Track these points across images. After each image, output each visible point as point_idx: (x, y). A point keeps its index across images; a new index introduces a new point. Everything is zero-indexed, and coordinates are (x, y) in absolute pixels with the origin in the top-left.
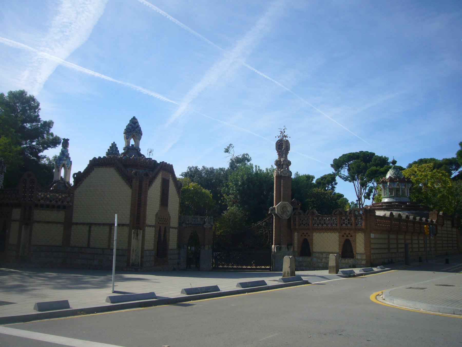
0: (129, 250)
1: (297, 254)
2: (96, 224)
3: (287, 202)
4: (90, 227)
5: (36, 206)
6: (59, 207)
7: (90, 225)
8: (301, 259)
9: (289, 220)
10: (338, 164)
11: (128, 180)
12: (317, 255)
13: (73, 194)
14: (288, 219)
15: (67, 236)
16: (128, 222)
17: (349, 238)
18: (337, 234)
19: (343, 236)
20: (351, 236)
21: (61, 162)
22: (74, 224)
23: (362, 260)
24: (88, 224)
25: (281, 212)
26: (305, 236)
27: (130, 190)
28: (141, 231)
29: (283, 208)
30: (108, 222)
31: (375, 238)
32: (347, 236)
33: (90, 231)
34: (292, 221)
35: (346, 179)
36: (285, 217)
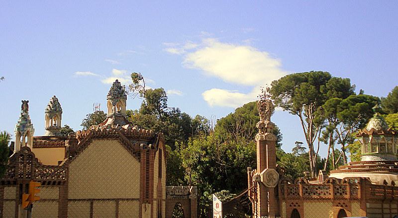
2: (97, 200)
3: (273, 169)
4: (92, 204)
6: (54, 183)
7: (92, 201)
9: (276, 188)
10: (278, 88)
11: (137, 154)
13: (68, 168)
14: (275, 188)
16: (138, 196)
21: (25, 129)
24: (89, 200)
25: (268, 180)
26: (295, 206)
27: (139, 164)
28: (150, 205)
29: (269, 175)
31: (370, 208)
33: (92, 208)
34: (279, 190)
35: (287, 108)
36: (272, 185)
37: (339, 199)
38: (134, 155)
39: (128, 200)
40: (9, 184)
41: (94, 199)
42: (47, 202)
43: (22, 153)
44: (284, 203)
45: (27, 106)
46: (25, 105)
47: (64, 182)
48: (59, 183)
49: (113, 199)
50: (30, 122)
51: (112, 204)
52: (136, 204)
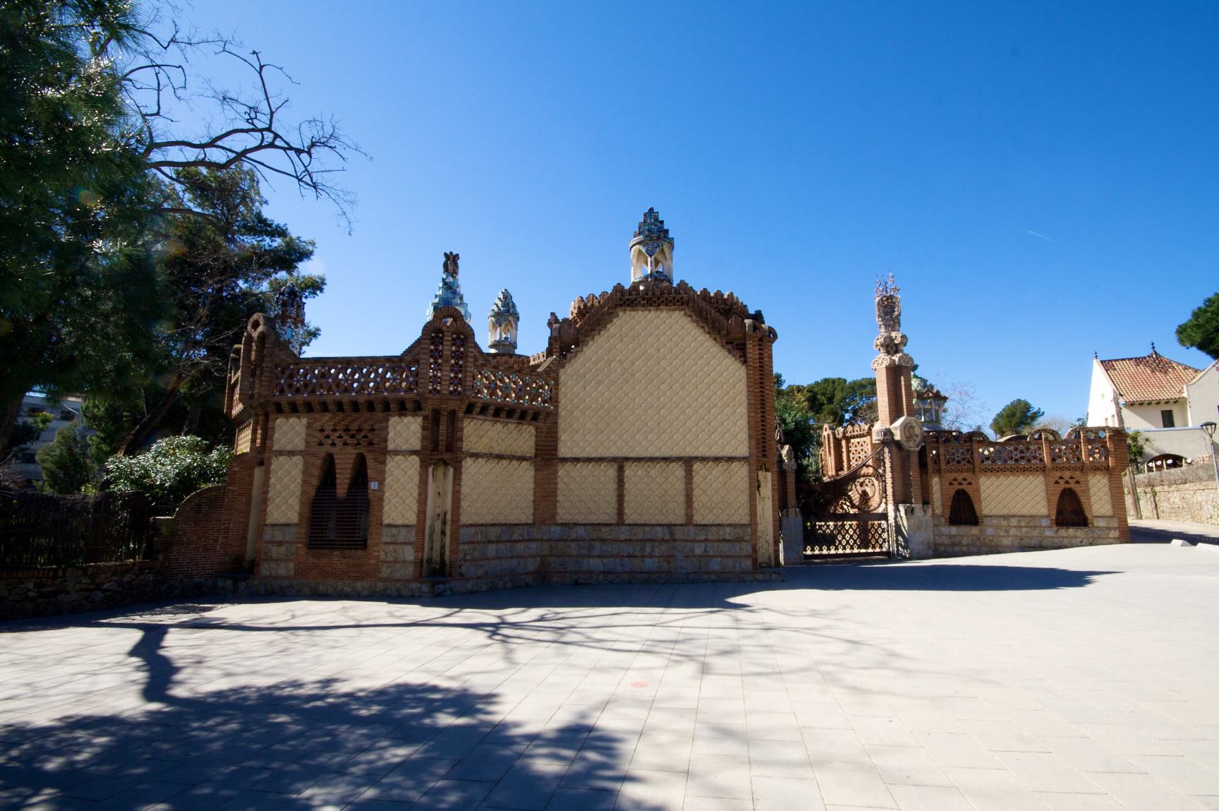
0: (753, 524)
1: (943, 520)
2: (639, 459)
4: (621, 470)
5: (469, 410)
7: (620, 463)
8: (954, 530)
12: (995, 521)
15: (545, 494)
16: (743, 450)
17: (1072, 485)
18: (1041, 478)
19: (1057, 482)
20: (1078, 482)
22: (565, 460)
23: (1109, 528)
30: (677, 452)
32: (1067, 482)
37: (1062, 469)
38: (730, 346)
39: (717, 459)
40: (402, 409)
41: (627, 459)
42: (505, 462)
43: (437, 324)
44: (935, 481)
45: (456, 265)
46: (451, 262)
47: (548, 414)
48: (535, 417)
49: (678, 459)
50: (461, 298)
51: (678, 471)
52: (740, 473)
